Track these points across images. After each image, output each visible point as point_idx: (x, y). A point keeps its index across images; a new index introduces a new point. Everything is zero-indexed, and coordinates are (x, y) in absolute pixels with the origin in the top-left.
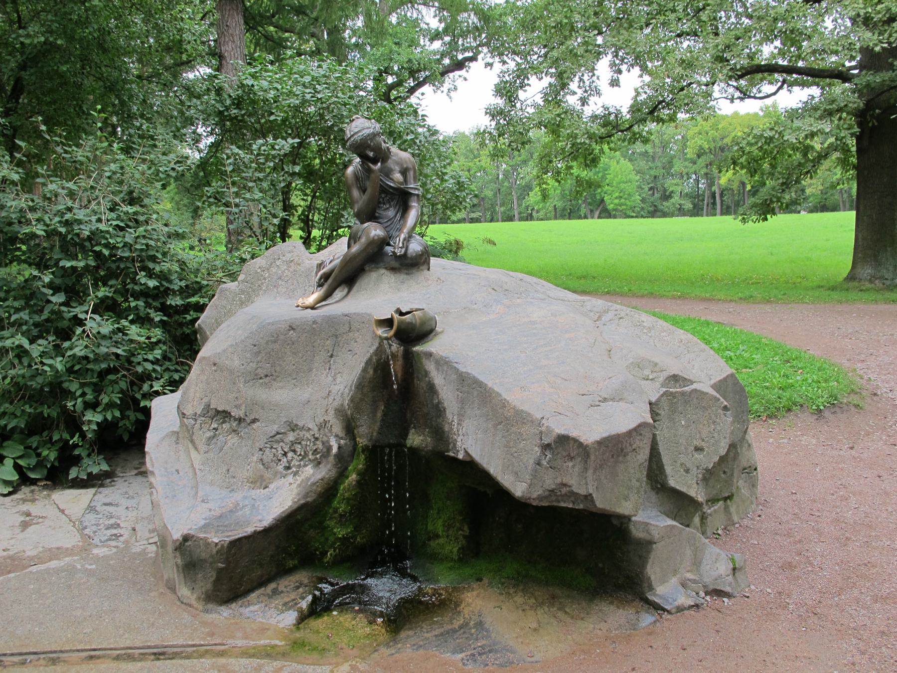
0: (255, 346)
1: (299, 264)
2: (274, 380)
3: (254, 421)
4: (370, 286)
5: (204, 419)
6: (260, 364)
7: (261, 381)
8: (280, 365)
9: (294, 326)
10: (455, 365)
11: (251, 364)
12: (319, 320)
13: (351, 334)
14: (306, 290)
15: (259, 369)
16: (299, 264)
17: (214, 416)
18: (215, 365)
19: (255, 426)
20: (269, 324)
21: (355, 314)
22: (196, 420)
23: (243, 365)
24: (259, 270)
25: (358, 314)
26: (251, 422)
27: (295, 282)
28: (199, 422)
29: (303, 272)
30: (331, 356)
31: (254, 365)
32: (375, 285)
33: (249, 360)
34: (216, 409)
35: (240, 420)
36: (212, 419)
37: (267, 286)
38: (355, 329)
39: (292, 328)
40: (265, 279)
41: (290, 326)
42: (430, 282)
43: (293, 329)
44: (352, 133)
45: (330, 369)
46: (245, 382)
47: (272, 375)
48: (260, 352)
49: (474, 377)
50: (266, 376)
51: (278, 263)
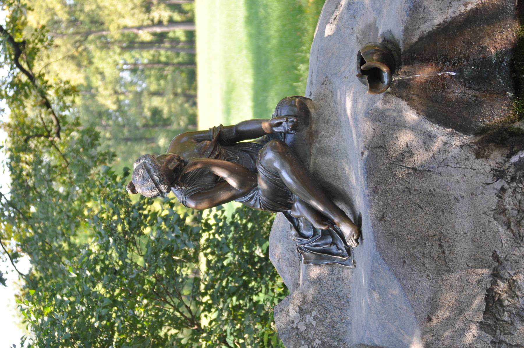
0: (405, 262)
2: (445, 237)
3: (496, 257)
4: (332, 161)
5: (498, 331)
7: (447, 252)
9: (380, 216)
11: (427, 265)
12: (372, 185)
14: (338, 279)
15: (433, 255)
17: (494, 316)
19: (502, 256)
20: (378, 247)
22: (501, 342)
23: (428, 276)
26: (498, 261)
28: (502, 338)
32: (331, 155)
33: (422, 268)
34: (485, 313)
35: (496, 276)
36: (498, 319)
37: (334, 338)
39: (382, 218)
40: (323, 343)
42: (327, 92)
46: (449, 271)
47: (440, 240)
48: (412, 256)
50: (441, 246)
51: (302, 328)
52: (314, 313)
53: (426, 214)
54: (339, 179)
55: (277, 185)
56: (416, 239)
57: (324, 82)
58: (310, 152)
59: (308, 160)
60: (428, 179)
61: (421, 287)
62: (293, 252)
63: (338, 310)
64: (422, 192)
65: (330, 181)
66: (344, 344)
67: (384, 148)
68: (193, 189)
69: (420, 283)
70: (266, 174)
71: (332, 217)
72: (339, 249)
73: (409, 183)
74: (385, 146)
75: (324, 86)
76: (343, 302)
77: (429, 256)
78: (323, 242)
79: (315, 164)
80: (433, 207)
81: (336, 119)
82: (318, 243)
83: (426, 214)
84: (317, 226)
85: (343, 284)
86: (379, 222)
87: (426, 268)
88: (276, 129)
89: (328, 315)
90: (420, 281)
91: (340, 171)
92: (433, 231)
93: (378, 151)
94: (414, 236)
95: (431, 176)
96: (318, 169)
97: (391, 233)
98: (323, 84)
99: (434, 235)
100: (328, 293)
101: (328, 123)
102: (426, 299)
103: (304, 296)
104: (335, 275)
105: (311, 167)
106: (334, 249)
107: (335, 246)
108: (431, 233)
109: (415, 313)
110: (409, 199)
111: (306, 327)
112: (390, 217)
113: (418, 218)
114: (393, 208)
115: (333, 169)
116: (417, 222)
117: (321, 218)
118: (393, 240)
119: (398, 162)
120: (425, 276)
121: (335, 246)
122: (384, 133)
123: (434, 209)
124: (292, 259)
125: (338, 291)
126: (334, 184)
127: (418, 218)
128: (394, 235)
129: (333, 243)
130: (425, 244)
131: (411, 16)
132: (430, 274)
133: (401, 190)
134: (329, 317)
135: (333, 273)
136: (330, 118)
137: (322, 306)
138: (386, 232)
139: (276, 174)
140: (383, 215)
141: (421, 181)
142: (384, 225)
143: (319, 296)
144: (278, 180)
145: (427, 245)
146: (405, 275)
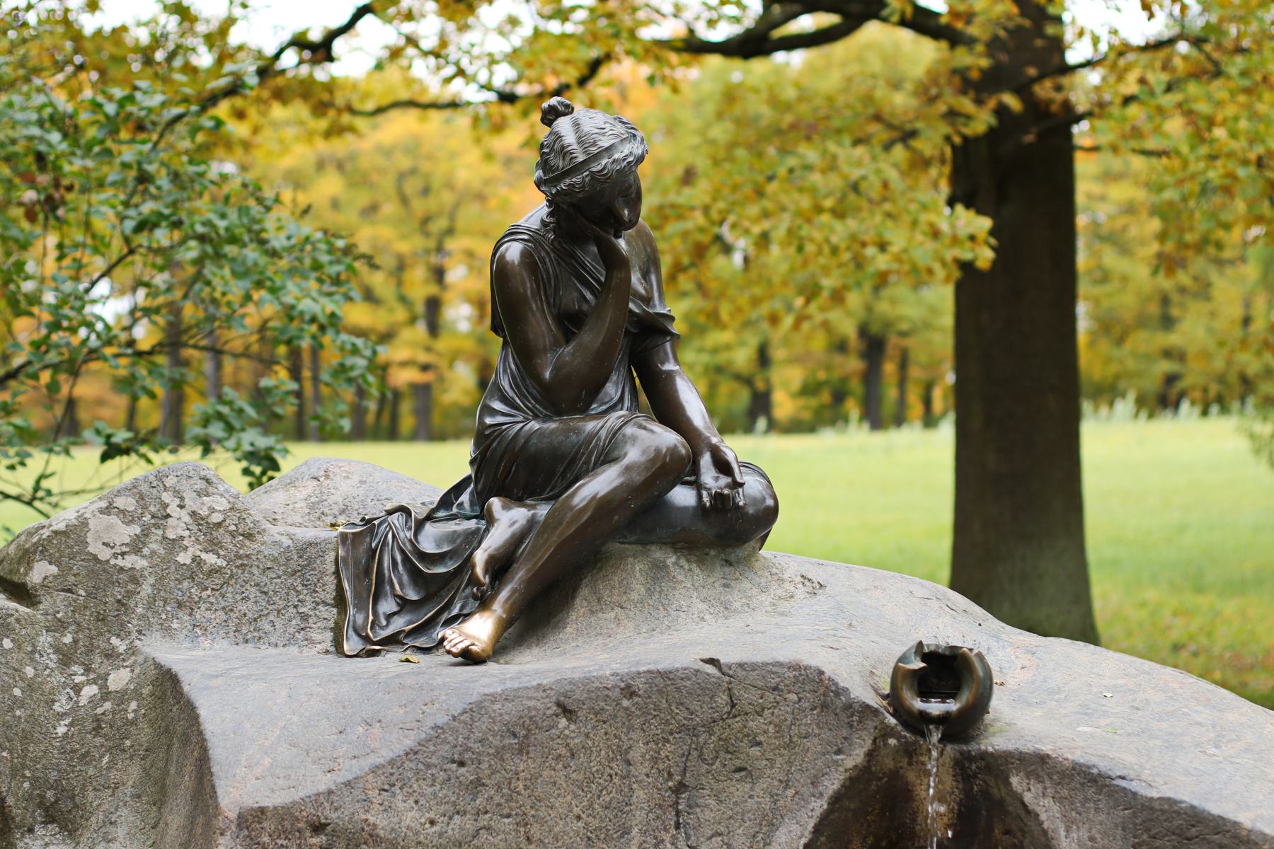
1: (249, 536)
4: (634, 596)
6: (484, 820)
8: (542, 822)
10: (1123, 783)
12: (640, 684)
13: (736, 724)
16: (249, 536)
18: (318, 828)
21: (741, 665)
23: (432, 823)
24: (104, 554)
25: (754, 667)
27: (253, 592)
29: (275, 560)
30: (680, 788)
31: (469, 824)
38: (749, 709)
41: (559, 704)
43: (566, 711)
44: (594, 150)
45: (677, 826)
48: (478, 784)
49: (1193, 807)
52: (211, 559)
53: (579, 818)
54: (592, 612)
55: (573, 461)
56: (519, 794)
57: (809, 580)
58: (652, 543)
59: (633, 538)
60: (658, 823)
61: (401, 805)
62: (342, 512)
63: (224, 617)
64: (627, 808)
65: (584, 592)
66: (140, 632)
67: (729, 713)
68: (547, 260)
69: (411, 801)
70: (603, 433)
71: (504, 594)
72: (389, 617)
73: (647, 775)
74: (735, 716)
75: (799, 578)
76: (244, 630)
77: (481, 825)
78: (405, 578)
79: (622, 557)
80: (593, 836)
81: (737, 605)
82: (400, 568)
83: (579, 818)
84: (480, 557)
85: (292, 630)
86: (554, 699)
87: (451, 818)
88: (706, 460)
89: (209, 592)
90: (416, 802)
91: (613, 615)
92: (537, 836)
93: (723, 699)
94: (526, 788)
95: (666, 830)
96: (612, 562)
97: (529, 730)
98: (802, 576)
99: (528, 839)
100: (266, 593)
101: (725, 586)
102: (372, 820)
103: (251, 535)
104: (315, 609)
105: (614, 546)
106: (387, 606)
107: (395, 609)
108: (535, 830)
109: (330, 792)
110: (611, 776)
111: (173, 540)
112: (567, 728)
113: (569, 798)
114: (587, 736)
115: (615, 598)
116: (559, 795)
117: (501, 566)
118: (514, 735)
119: (696, 749)
120: (432, 815)
121: (395, 609)
122: (766, 712)
123: (589, 839)
124: (326, 511)
125: (271, 617)
126: (578, 601)
127: (569, 798)
128: (526, 737)
129: (404, 604)
130: (508, 816)
131: (1074, 769)
132: (436, 828)
133: (630, 756)
134: (204, 594)
135: (318, 604)
136: (736, 592)
137: (232, 576)
138: (531, 718)
139: (607, 456)
140: (570, 712)
141: (653, 805)
142: (549, 712)
143: (255, 570)
144: (587, 462)
145: (506, 820)
146: (428, 766)
